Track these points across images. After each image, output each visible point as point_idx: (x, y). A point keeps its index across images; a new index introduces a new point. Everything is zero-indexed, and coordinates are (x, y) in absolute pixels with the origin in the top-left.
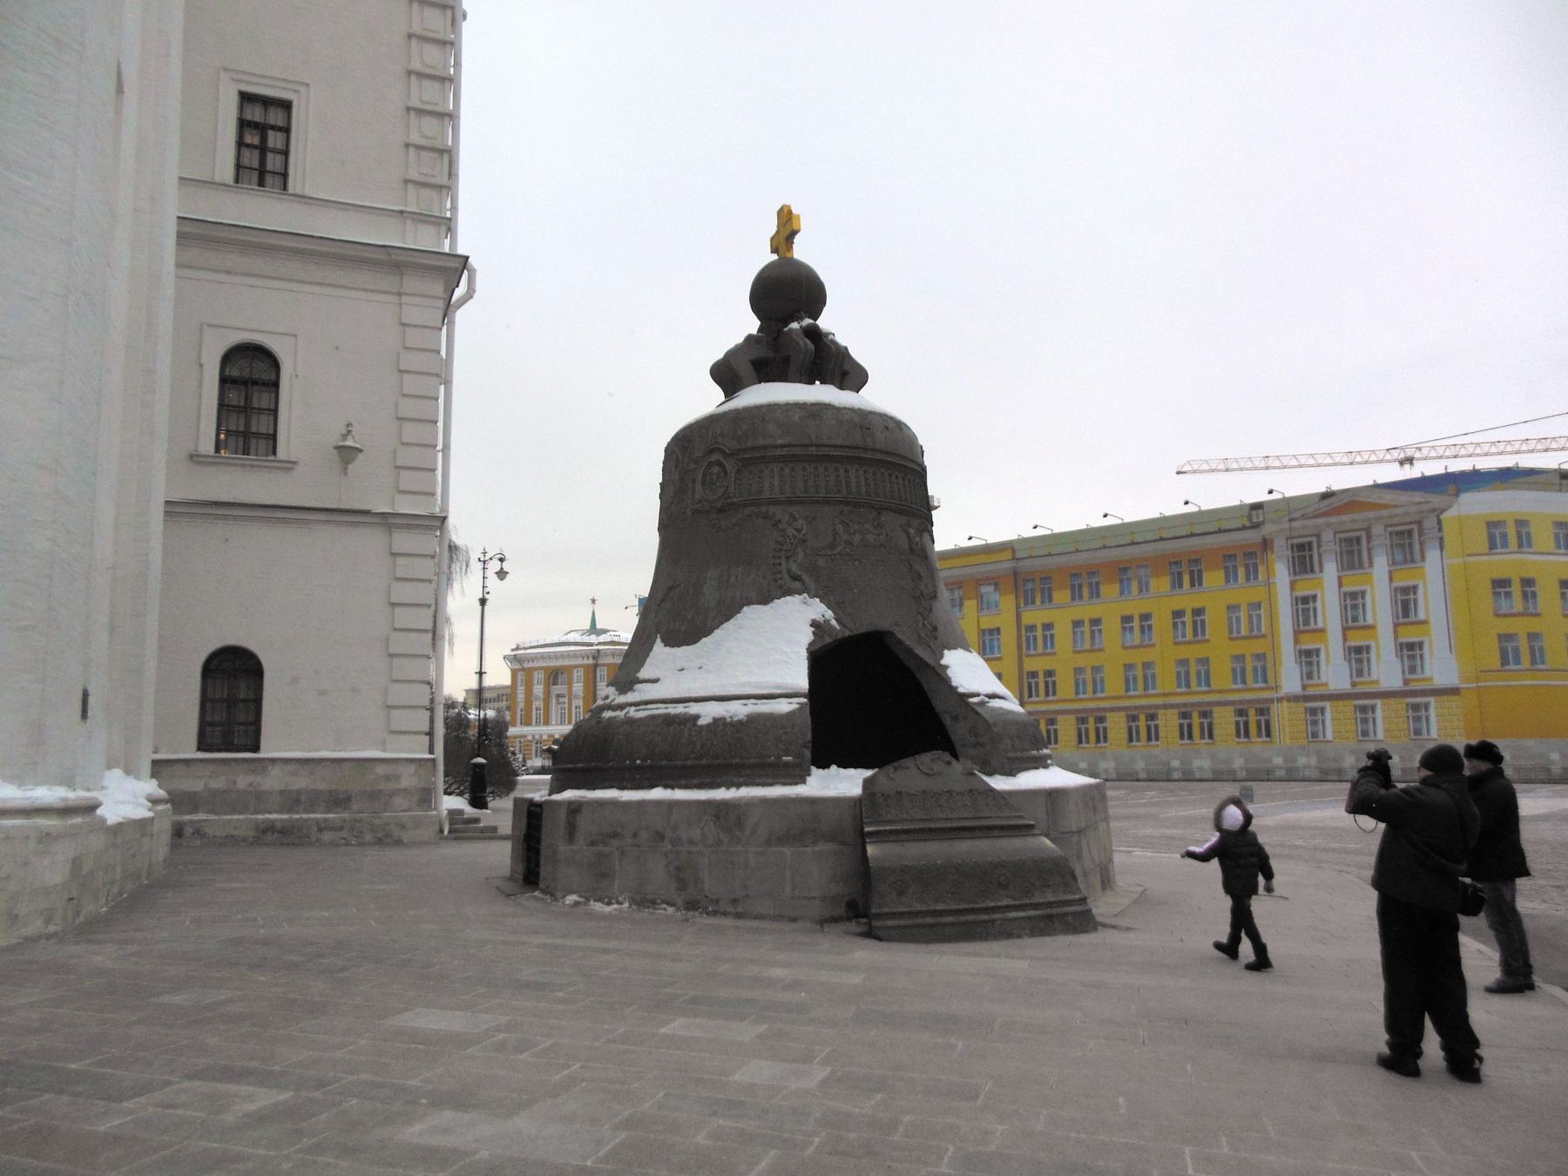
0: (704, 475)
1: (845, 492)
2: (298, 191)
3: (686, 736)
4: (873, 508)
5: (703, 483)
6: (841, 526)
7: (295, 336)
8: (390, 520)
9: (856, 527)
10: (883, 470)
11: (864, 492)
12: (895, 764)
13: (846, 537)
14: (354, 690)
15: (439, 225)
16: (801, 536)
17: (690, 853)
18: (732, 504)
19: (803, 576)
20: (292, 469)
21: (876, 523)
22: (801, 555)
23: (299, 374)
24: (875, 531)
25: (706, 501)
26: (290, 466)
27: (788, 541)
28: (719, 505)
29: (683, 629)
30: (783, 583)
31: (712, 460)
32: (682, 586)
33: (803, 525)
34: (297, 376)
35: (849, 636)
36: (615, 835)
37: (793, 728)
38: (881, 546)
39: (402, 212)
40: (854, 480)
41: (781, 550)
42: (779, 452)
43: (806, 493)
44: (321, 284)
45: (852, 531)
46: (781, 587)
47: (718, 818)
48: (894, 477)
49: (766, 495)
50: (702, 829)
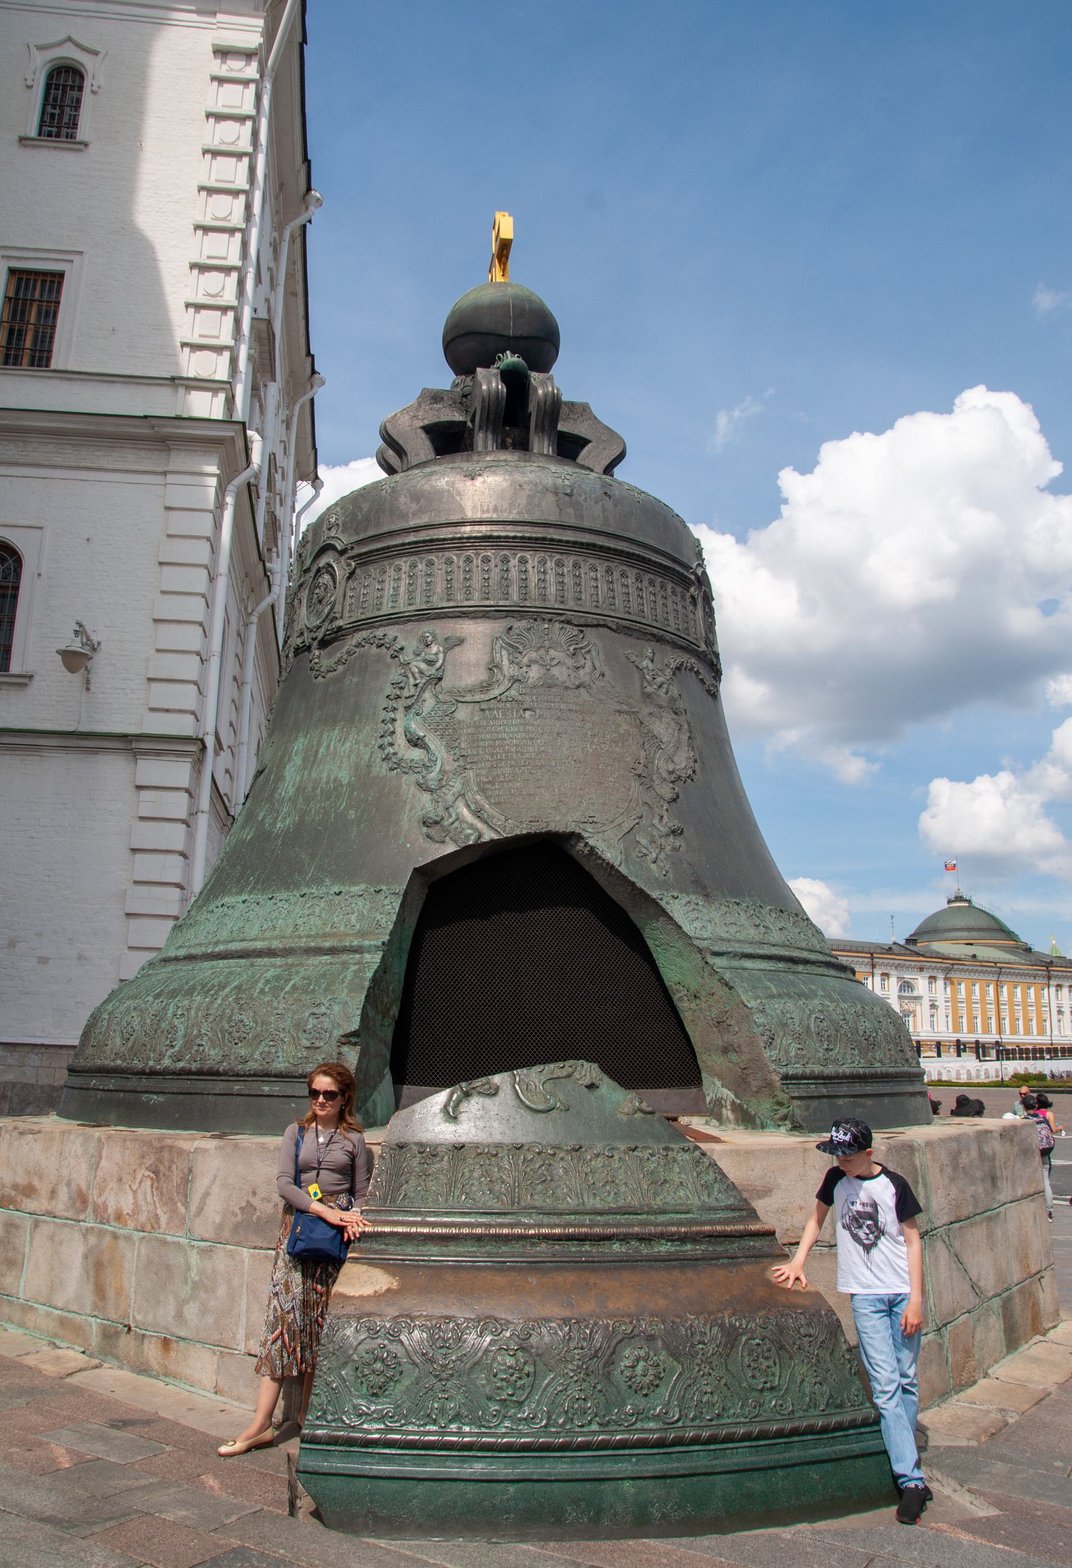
0: (311, 593)
1: (515, 596)
2: (61, 367)
3: (170, 1015)
4: (569, 622)
5: (310, 599)
6: (504, 652)
7: (41, 528)
8: (134, 745)
9: (533, 655)
10: (591, 561)
11: (552, 598)
12: (464, 1084)
13: (508, 669)
14: (80, 957)
15: (215, 391)
16: (432, 671)
17: (115, 1236)
18: (340, 629)
19: (426, 740)
20: (25, 685)
21: (571, 648)
22: (429, 702)
23: (42, 573)
24: (570, 662)
25: (308, 628)
26: (24, 681)
27: (412, 681)
28: (320, 635)
29: (249, 837)
30: (392, 751)
31: (321, 565)
32: (266, 771)
33: (436, 654)
34: (39, 575)
35: (492, 841)
36: (29, 1191)
37: (329, 1008)
38: (578, 687)
39: (173, 379)
40: (533, 578)
41: (399, 697)
42: (411, 538)
43: (449, 600)
44: (78, 468)
45: (525, 660)
46: (386, 759)
47: (156, 1172)
48: (616, 575)
49: (386, 609)
50: (135, 1192)
